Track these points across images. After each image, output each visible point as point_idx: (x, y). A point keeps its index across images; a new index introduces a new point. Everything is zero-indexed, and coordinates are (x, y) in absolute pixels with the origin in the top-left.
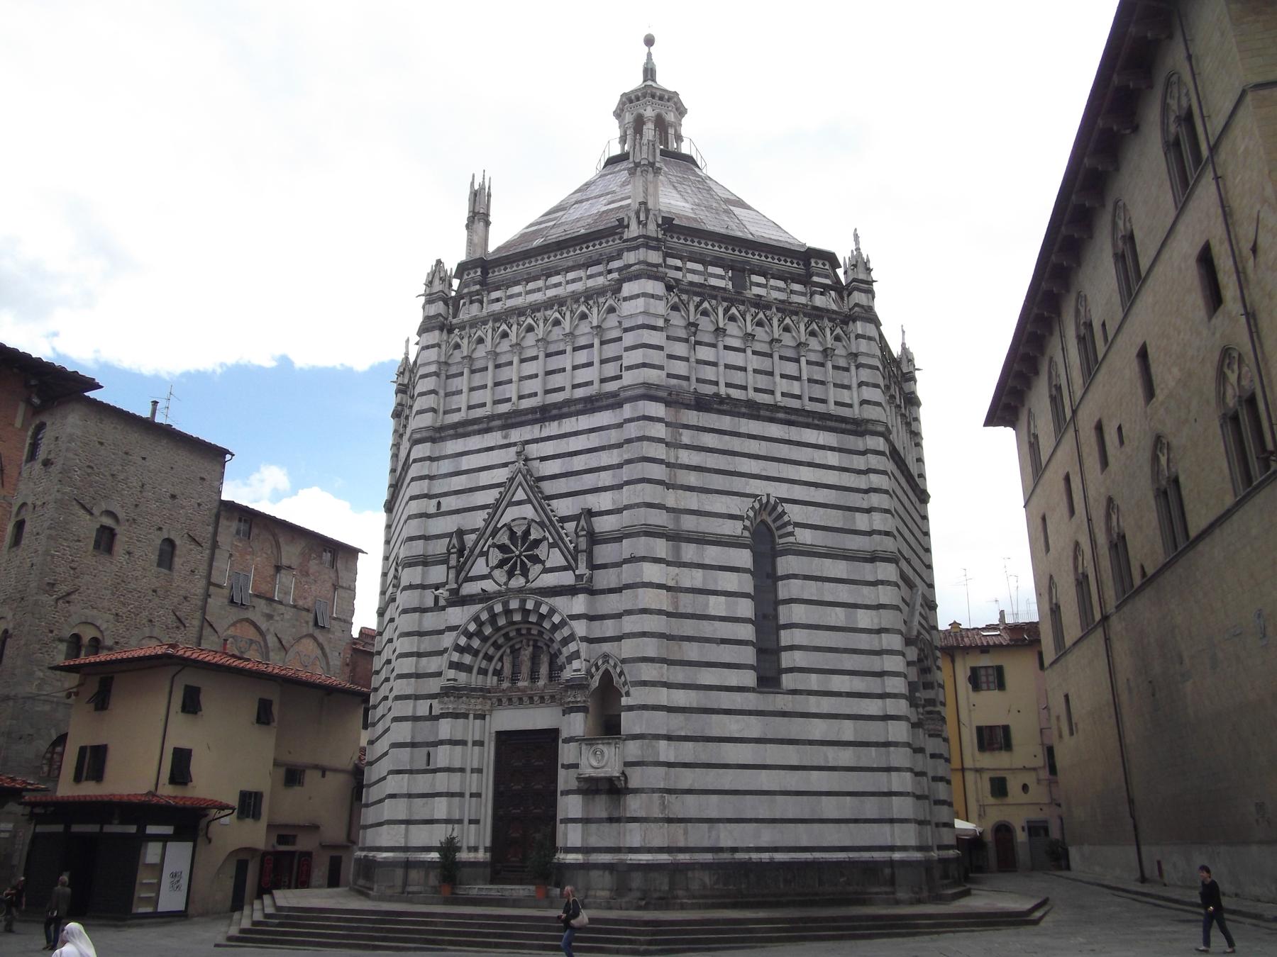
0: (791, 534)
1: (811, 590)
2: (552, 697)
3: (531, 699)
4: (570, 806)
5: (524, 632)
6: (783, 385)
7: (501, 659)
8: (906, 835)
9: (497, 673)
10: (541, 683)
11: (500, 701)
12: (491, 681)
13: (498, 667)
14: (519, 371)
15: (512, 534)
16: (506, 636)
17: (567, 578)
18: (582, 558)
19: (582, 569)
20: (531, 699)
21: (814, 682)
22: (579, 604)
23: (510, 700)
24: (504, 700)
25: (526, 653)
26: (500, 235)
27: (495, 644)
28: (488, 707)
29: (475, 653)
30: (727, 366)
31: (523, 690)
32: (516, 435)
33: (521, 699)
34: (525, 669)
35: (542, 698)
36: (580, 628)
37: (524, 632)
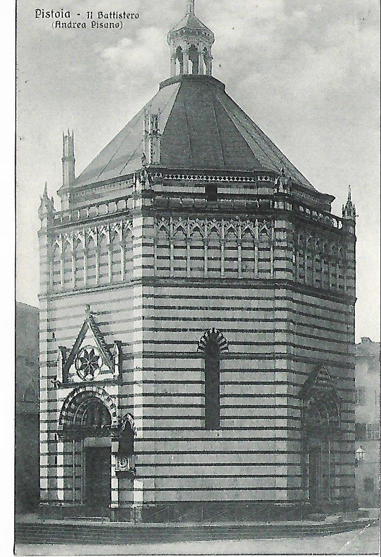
0: (227, 348)
1: (236, 377)
4: (115, 483)
6: (224, 264)
8: (283, 495)
14: (87, 263)
15: (86, 352)
17: (110, 376)
18: (117, 368)
19: (117, 373)
21: (236, 423)
22: (113, 390)
26: (80, 168)
29: (74, 411)
30: (192, 258)
32: (86, 299)
36: (116, 402)
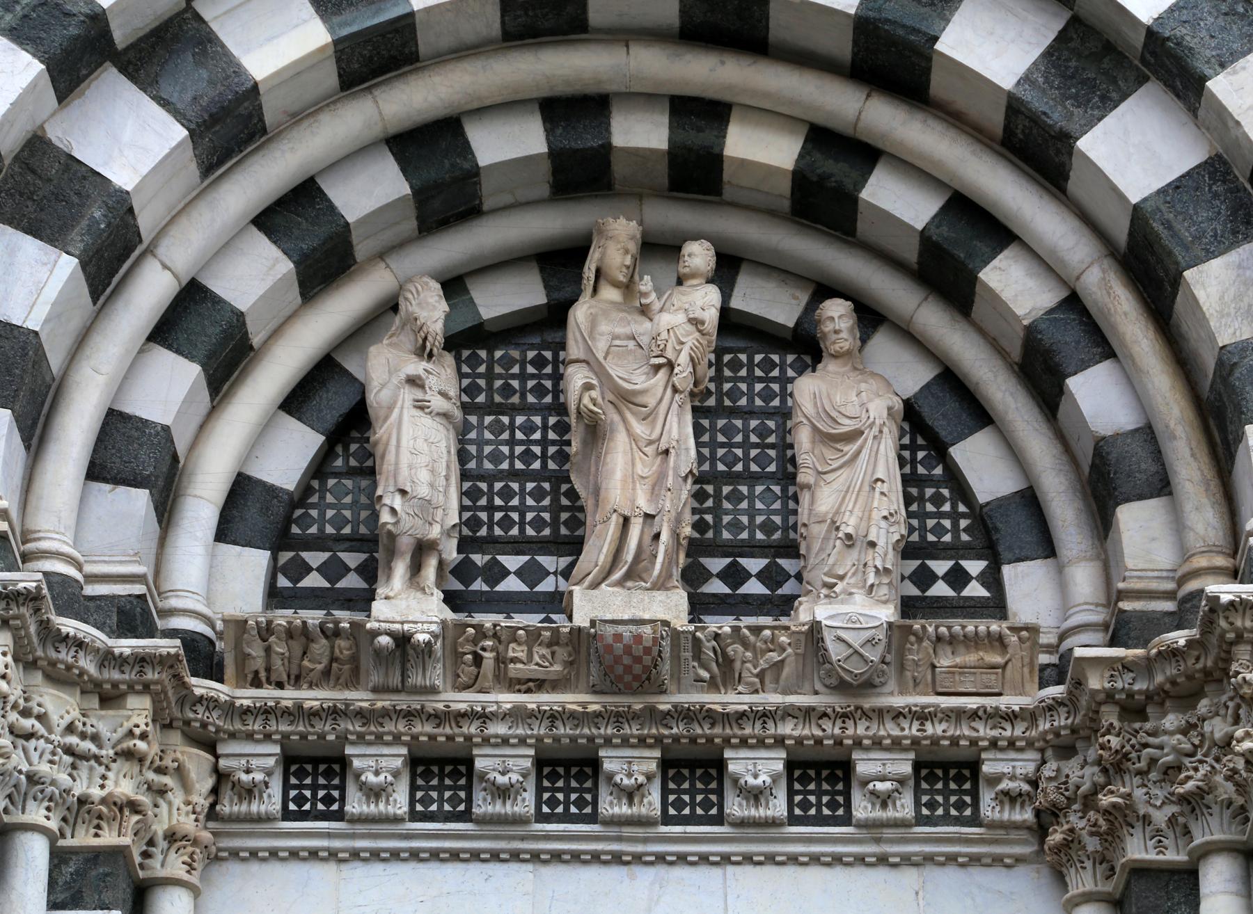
2: (947, 774)
3: (695, 772)
5: (641, 133)
7: (334, 403)
9: (248, 511)
10: (851, 610)
11: (317, 772)
12: (215, 581)
13: (288, 457)
16: (429, 149)
20: (695, 772)
23: (443, 771)
24: (378, 763)
25: (644, 337)
27: (296, 216)
28: (178, 812)
31: (623, 666)
33: (568, 772)
34: (641, 473)
35: (821, 776)
37: (641, 133)
